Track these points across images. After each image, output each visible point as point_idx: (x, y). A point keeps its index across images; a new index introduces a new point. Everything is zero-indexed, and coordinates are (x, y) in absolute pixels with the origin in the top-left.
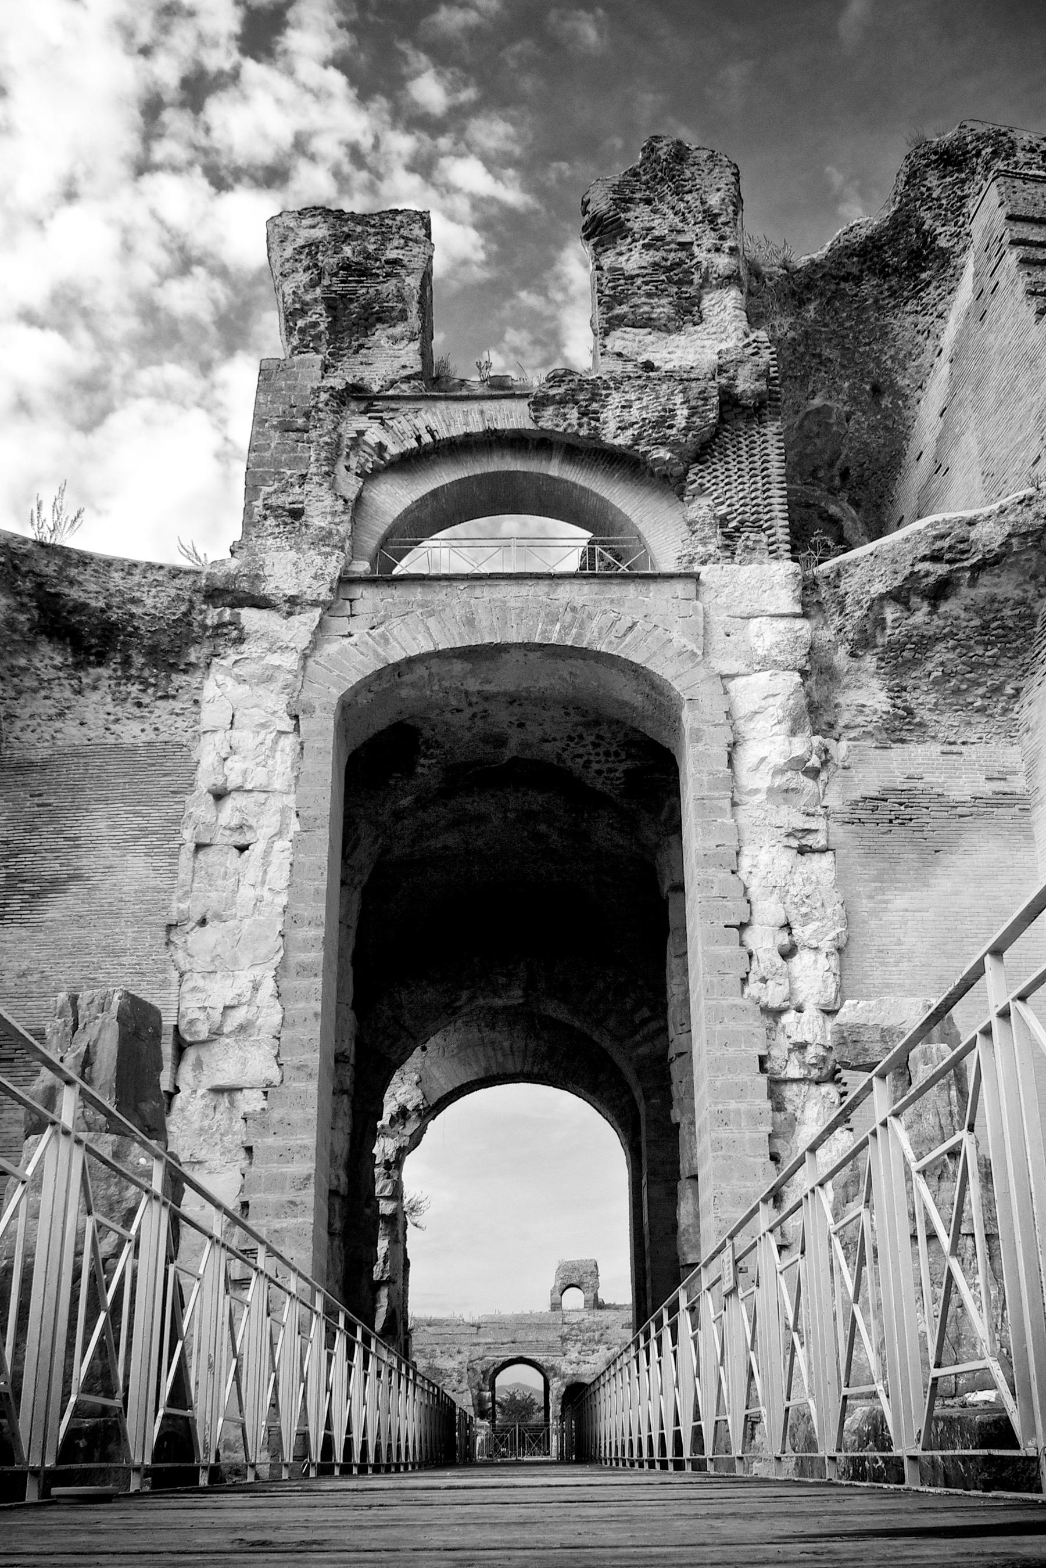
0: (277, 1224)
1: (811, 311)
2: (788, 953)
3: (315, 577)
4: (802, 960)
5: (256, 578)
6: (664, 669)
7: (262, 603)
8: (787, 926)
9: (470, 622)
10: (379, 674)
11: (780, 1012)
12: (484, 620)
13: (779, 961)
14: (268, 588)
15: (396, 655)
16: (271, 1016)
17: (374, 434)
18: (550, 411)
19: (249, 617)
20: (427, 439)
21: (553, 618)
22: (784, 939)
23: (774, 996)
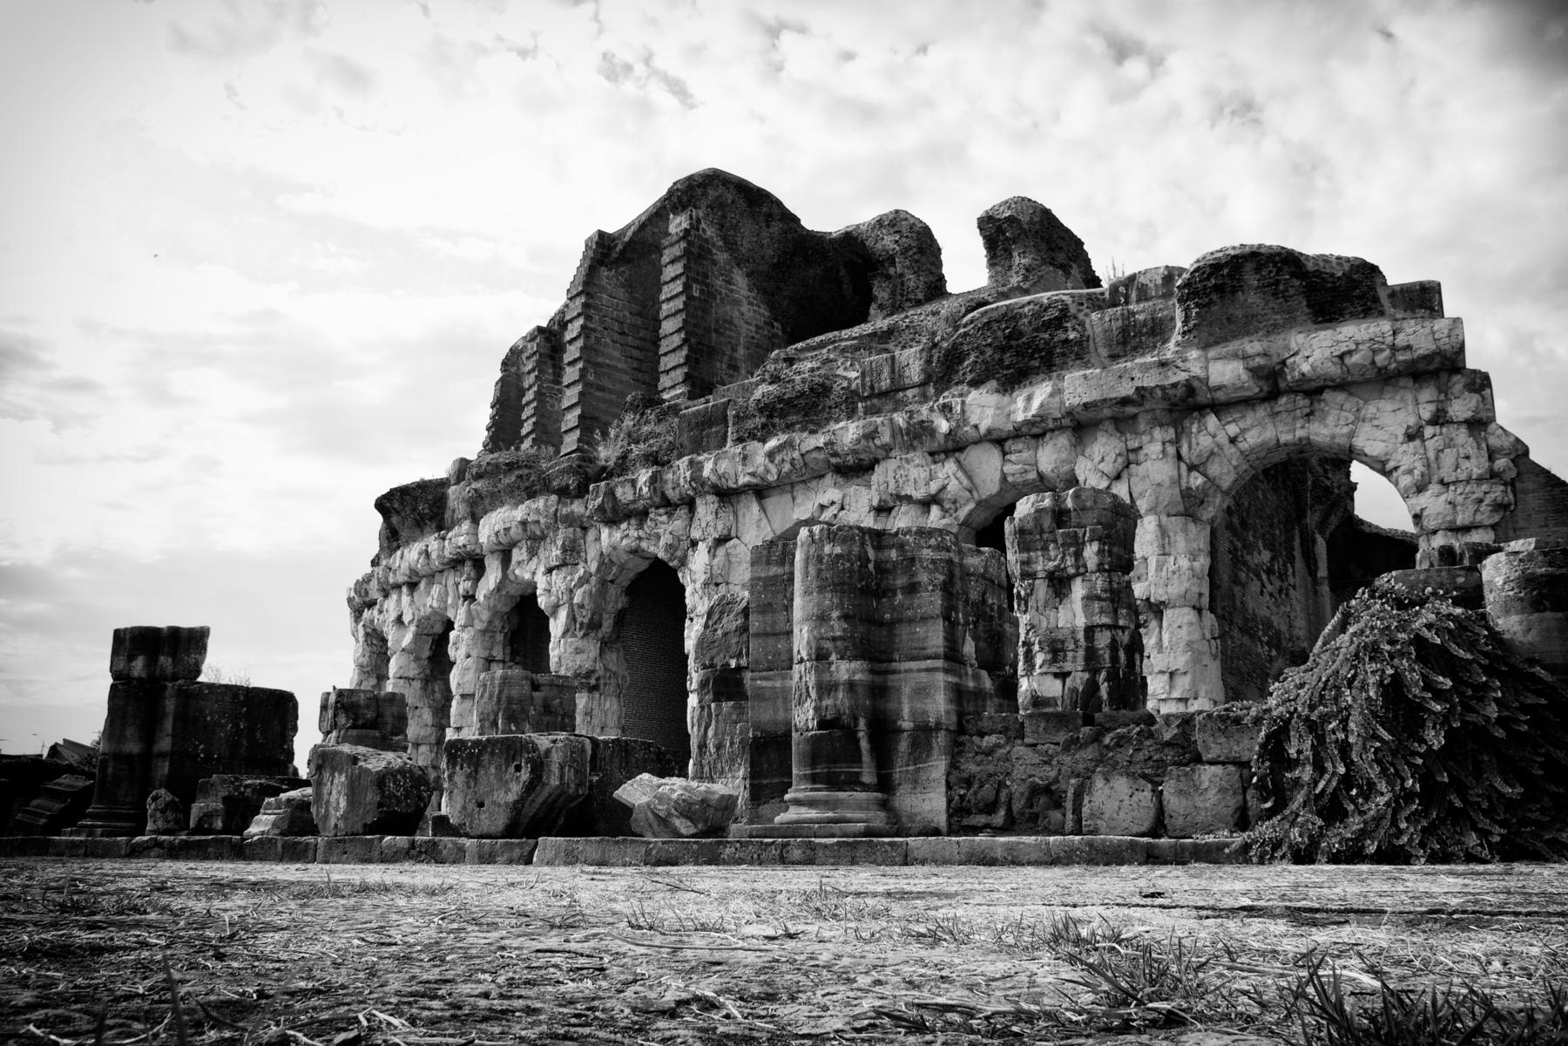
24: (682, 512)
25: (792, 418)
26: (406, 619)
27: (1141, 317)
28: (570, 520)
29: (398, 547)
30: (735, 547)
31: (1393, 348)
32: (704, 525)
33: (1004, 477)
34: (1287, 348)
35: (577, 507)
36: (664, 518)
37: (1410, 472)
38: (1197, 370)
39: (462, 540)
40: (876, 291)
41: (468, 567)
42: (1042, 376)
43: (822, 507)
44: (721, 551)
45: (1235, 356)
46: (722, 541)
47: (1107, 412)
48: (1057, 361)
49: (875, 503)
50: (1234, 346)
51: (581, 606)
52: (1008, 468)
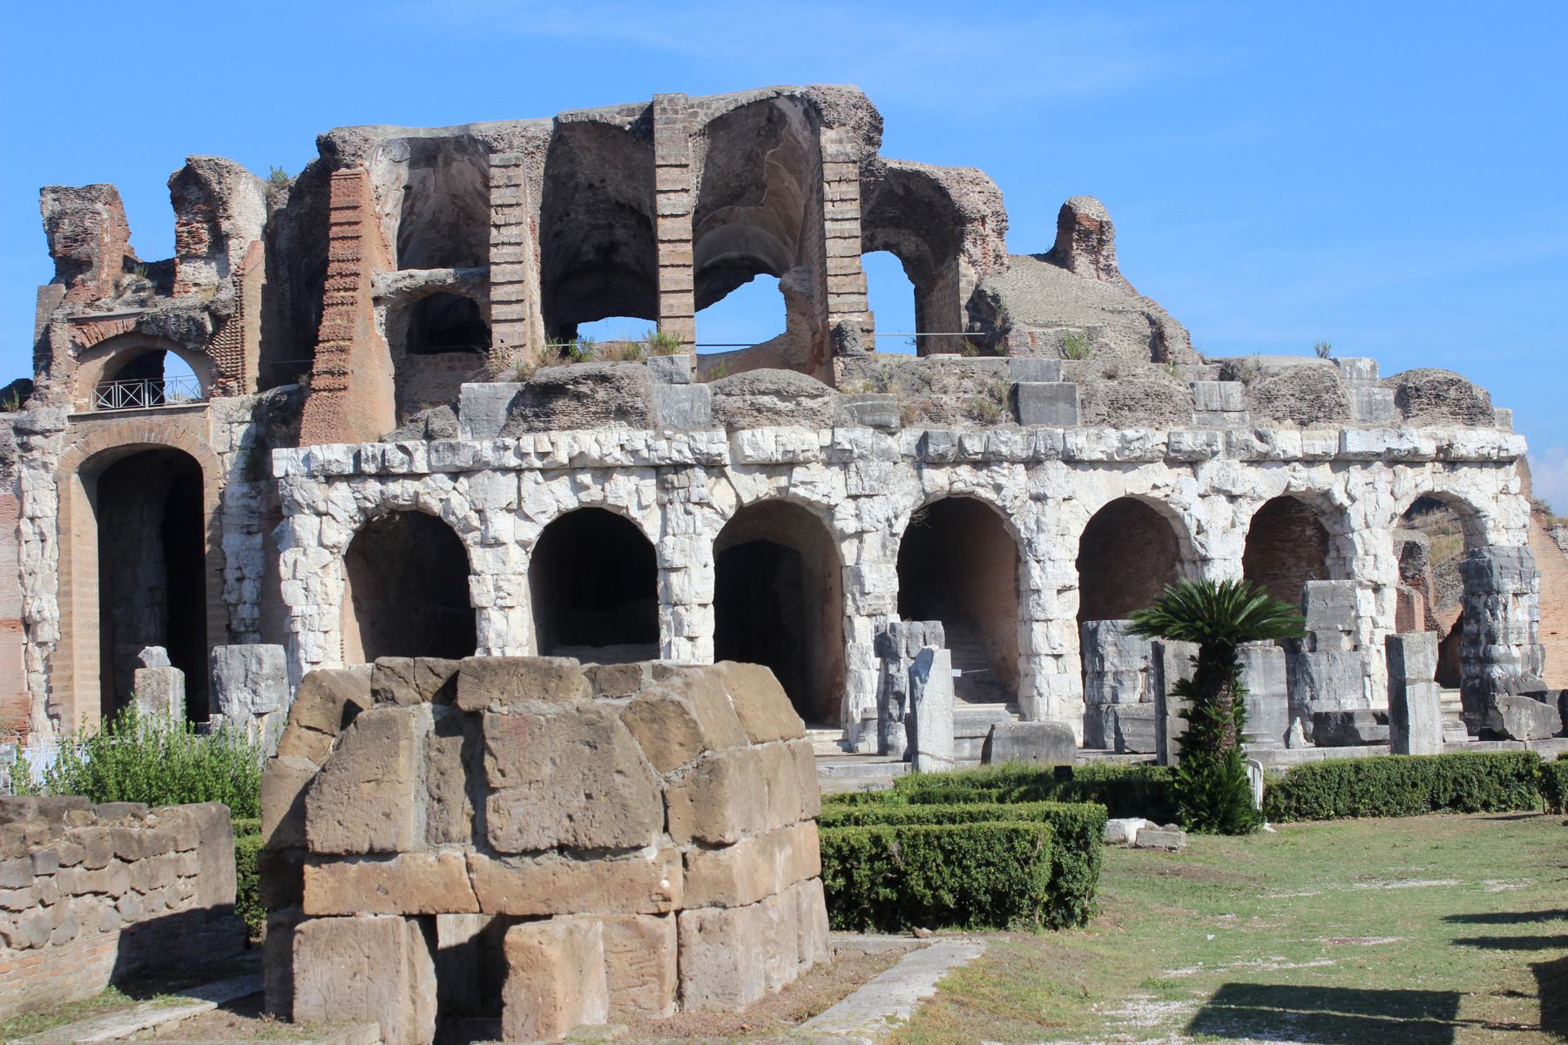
0: (63, 694)
1: (308, 199)
2: (240, 580)
3: (57, 419)
4: (246, 583)
5: (33, 422)
6: (195, 453)
7: (36, 433)
8: (239, 568)
9: (120, 434)
10: (88, 459)
11: (236, 605)
12: (126, 433)
13: (236, 584)
14: (37, 428)
15: (93, 451)
16: (57, 614)
17: (81, 339)
18: (144, 327)
19: (35, 440)
20: (101, 339)
21: (151, 431)
22: (238, 574)
23: (232, 598)
24: (1020, 468)
25: (1141, 414)
26: (529, 508)
27: (1379, 397)
28: (885, 455)
29: (547, 430)
30: (1076, 506)
31: (1500, 449)
32: (1054, 486)
33: (1289, 486)
34: (1455, 437)
35: (890, 442)
36: (1006, 472)
37: (1494, 520)
38: (1417, 445)
39: (714, 449)
40: (968, 245)
41: (700, 473)
42: (1323, 425)
43: (1155, 487)
44: (1065, 506)
45: (1433, 437)
46: (1070, 499)
47: (1360, 458)
48: (1334, 416)
49: (1202, 492)
50: (1429, 429)
51: (893, 535)
52: (1294, 482)
